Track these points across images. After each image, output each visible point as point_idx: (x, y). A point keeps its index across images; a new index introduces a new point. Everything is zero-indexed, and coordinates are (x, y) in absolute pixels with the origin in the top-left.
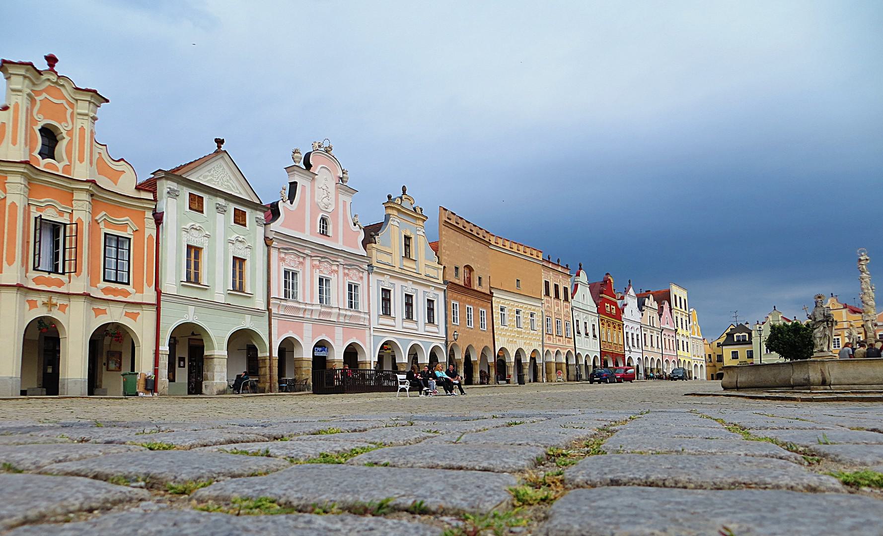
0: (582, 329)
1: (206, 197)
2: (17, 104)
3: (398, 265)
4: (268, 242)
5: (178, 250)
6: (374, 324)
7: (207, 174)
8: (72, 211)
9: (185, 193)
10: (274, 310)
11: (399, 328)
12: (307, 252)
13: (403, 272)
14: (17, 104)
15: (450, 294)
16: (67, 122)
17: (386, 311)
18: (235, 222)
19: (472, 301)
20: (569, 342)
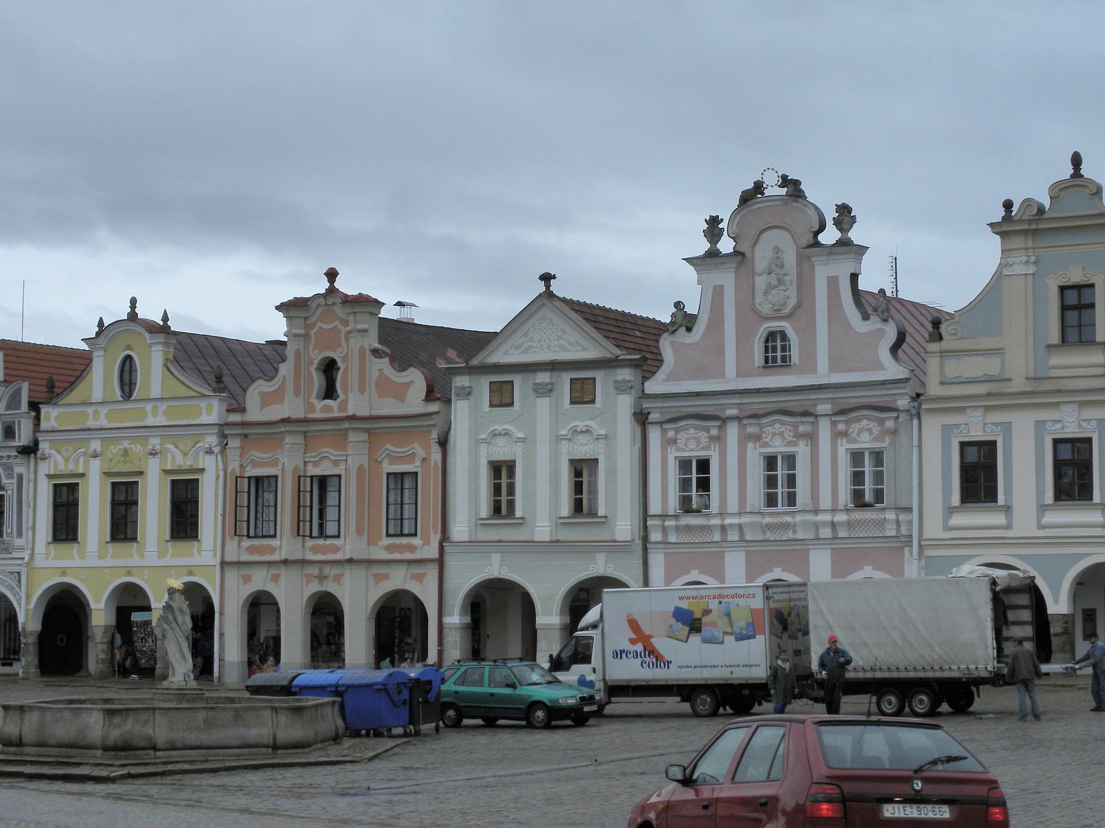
1: (517, 380)
4: (641, 418)
7: (523, 339)
8: (347, 456)
9: (483, 385)
13: (1046, 386)
16: (342, 347)
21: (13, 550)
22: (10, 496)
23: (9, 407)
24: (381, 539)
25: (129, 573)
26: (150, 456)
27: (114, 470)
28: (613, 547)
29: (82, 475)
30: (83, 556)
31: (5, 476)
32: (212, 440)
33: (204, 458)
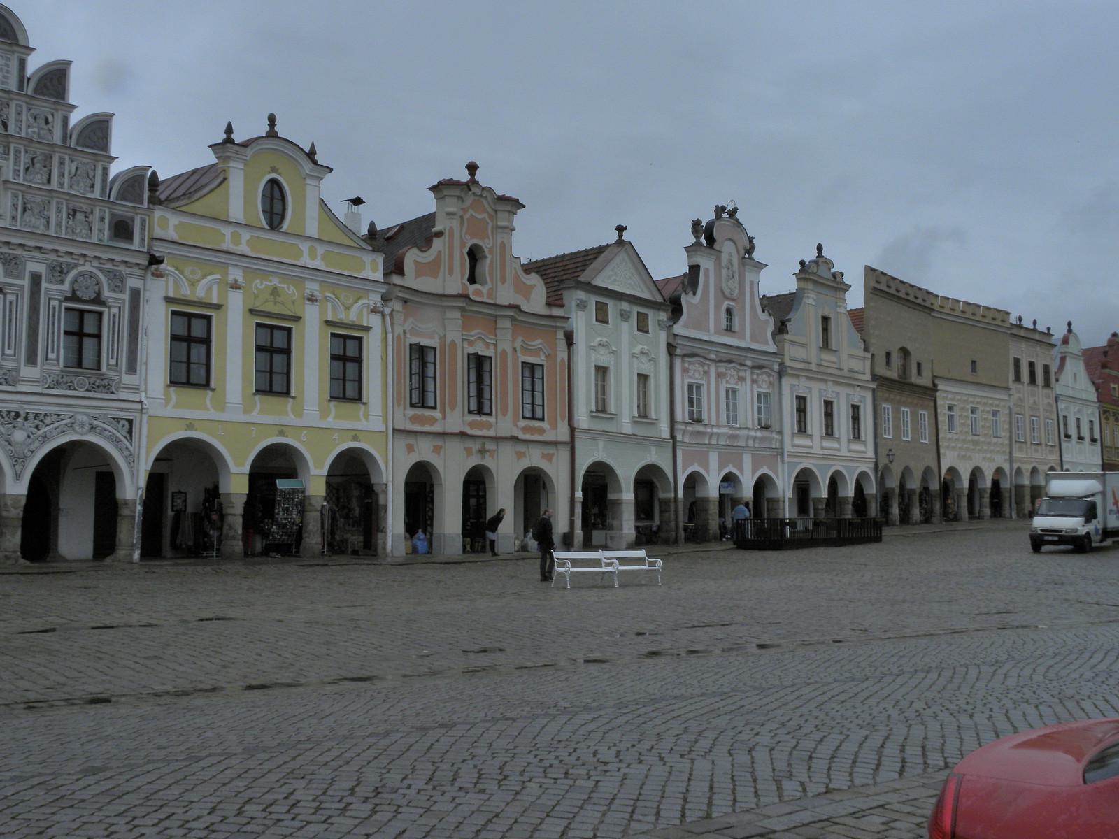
0: (1072, 431)
1: (612, 304)
2: (451, 228)
3: (814, 360)
4: (671, 348)
5: (588, 374)
6: (788, 447)
10: (679, 438)
11: (817, 450)
12: (713, 356)
13: (822, 370)
14: (451, 228)
15: (879, 394)
16: (489, 238)
17: (802, 428)
18: (639, 330)
19: (909, 400)
20: (1051, 453)
21: (117, 389)
22: (114, 316)
23: (123, 195)
24: (518, 421)
25: (281, 433)
26: (307, 302)
27: (262, 309)
28: (657, 442)
29: (218, 307)
30: (221, 405)
31: (109, 288)
32: (375, 299)
33: (368, 317)
